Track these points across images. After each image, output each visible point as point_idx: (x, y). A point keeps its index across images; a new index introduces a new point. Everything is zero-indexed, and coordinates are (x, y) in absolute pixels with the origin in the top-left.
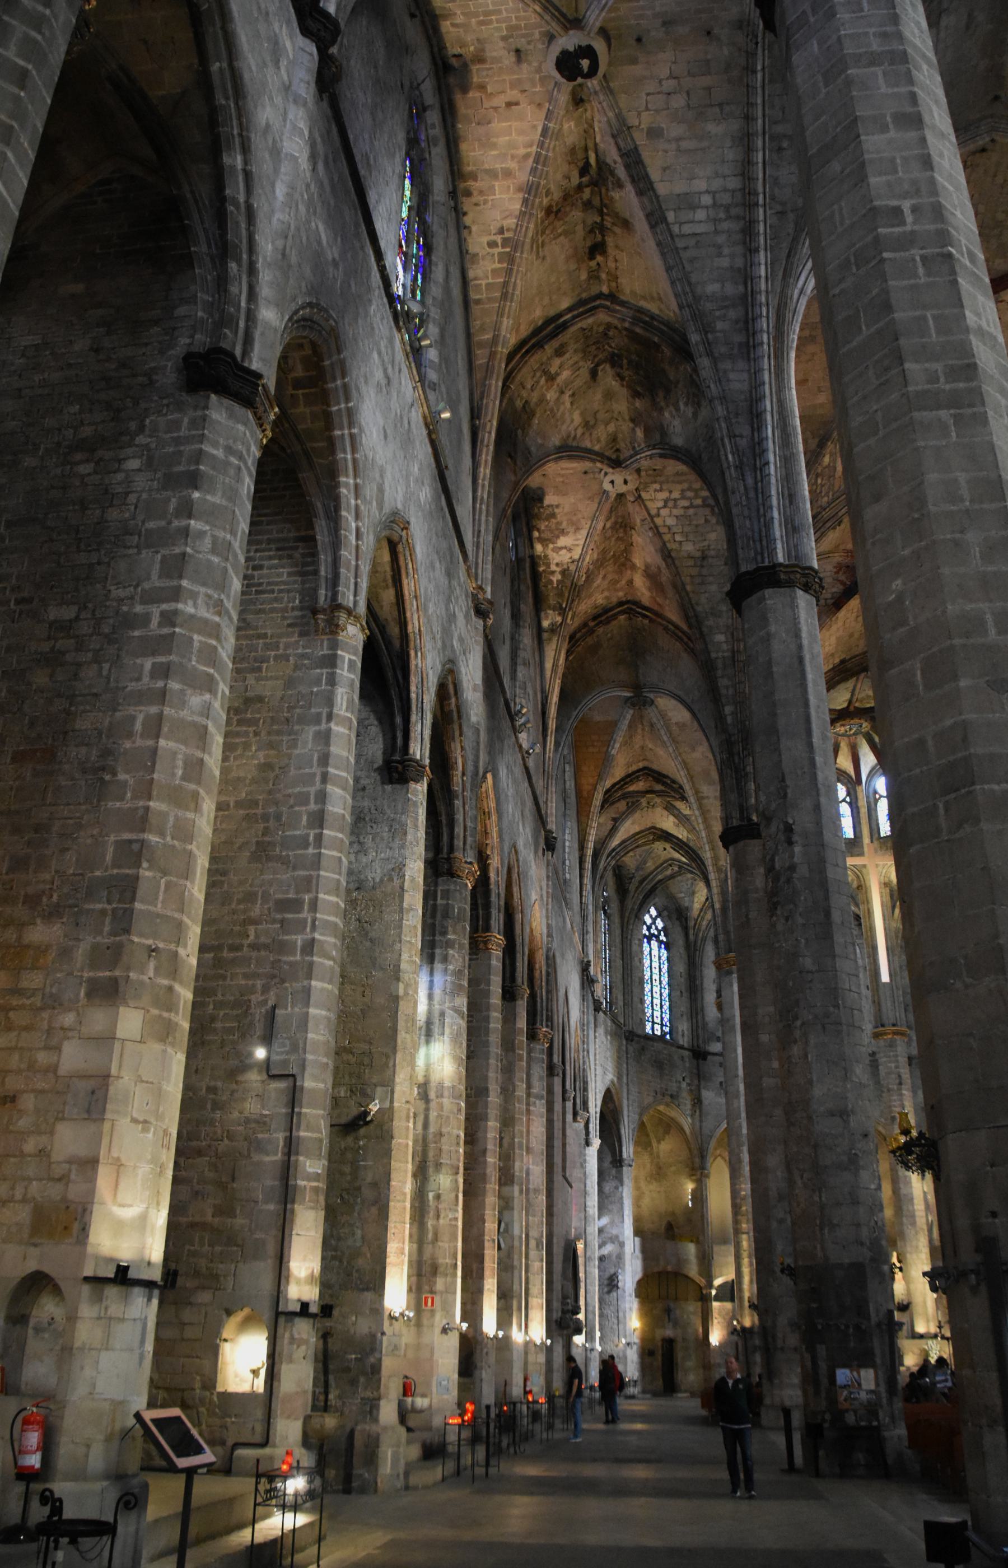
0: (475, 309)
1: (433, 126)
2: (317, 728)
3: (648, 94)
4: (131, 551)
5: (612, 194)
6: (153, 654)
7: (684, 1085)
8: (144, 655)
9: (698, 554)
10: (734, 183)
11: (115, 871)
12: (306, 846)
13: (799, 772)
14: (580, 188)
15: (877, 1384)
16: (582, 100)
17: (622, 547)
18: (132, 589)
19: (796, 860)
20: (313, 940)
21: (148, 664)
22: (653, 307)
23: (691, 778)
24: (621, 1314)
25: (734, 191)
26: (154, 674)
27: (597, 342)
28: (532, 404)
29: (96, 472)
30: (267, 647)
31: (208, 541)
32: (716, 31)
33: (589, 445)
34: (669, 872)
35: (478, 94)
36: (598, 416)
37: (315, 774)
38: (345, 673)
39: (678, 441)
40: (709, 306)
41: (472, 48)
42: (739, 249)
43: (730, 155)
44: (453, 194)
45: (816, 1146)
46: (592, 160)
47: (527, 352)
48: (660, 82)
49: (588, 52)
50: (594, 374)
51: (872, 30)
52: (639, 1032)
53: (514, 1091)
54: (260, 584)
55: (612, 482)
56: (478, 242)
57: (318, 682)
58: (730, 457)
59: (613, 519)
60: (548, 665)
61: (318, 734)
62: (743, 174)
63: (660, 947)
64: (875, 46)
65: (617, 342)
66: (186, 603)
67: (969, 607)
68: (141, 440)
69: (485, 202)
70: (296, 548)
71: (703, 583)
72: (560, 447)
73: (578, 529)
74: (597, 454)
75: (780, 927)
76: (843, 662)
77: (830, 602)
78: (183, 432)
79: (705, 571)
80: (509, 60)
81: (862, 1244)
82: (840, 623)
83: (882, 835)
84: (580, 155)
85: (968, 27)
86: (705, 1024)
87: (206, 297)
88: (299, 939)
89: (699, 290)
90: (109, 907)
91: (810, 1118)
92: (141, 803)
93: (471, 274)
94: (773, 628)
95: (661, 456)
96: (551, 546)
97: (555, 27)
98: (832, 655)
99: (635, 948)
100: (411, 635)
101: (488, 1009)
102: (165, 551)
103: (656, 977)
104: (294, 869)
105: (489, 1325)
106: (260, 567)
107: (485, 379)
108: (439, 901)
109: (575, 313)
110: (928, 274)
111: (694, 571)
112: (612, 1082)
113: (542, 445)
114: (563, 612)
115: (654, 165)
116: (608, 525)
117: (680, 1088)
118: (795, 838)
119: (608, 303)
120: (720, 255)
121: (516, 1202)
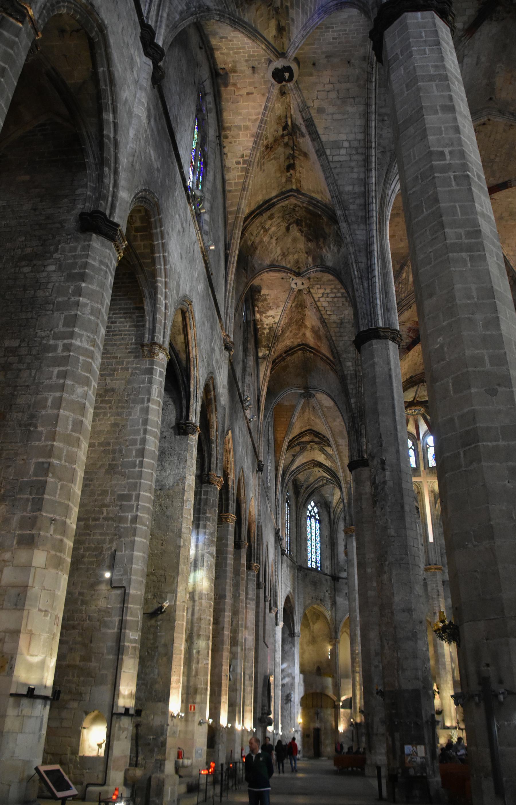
0: (229, 195)
1: (210, 103)
2: (142, 405)
3: (318, 91)
4: (49, 313)
5: (299, 140)
6: (58, 366)
7: (327, 594)
8: (54, 366)
9: (339, 321)
10: (360, 136)
11: (35, 478)
12: (135, 466)
13: (389, 433)
14: (283, 136)
15: (426, 753)
16: (285, 93)
17: (300, 317)
18: (48, 332)
19: (386, 478)
20: (137, 516)
21: (56, 370)
22: (318, 197)
23: (333, 435)
24: (292, 715)
25: (359, 141)
26: (58, 377)
27: (290, 213)
29: (32, 272)
30: (118, 363)
31: (89, 309)
32: (352, 61)
33: (284, 265)
34: (321, 483)
35: (232, 88)
36: (290, 250)
37: (140, 430)
38: (157, 378)
39: (330, 264)
40: (346, 197)
41: (230, 65)
42: (363, 169)
43: (358, 122)
44: (219, 137)
45: (395, 628)
46: (289, 123)
47: (254, 217)
48: (324, 85)
49: (289, 69)
50: (288, 229)
51: (430, 64)
52: (305, 566)
53: (239, 596)
54: (115, 331)
55: (296, 284)
56: (231, 161)
57: (143, 382)
58: (356, 273)
59: (296, 303)
60: (261, 375)
61: (142, 409)
62: (364, 132)
63: (316, 522)
64: (432, 72)
65: (300, 213)
66: (76, 340)
67: (476, 352)
68: (56, 256)
69: (235, 142)
70: (134, 313)
71: (340, 336)
72: (270, 266)
73: (278, 307)
74: (288, 269)
75: (378, 513)
76: (411, 377)
78: (78, 252)
79: (342, 330)
80: (249, 72)
81: (418, 679)
82: (410, 358)
83: (430, 466)
84: (283, 120)
85: (477, 64)
86: (338, 563)
87: (92, 185)
88: (130, 516)
89: (341, 189)
90: (31, 497)
91: (392, 613)
92: (50, 443)
93: (227, 177)
94: (376, 360)
95: (321, 271)
97: (272, 56)
98: (406, 374)
99: (303, 522)
100: (192, 359)
101: (227, 553)
102: (66, 313)
103: (313, 537)
104: (128, 479)
105: (224, 721)
106: (115, 322)
107: (233, 230)
108: (203, 497)
109: (279, 198)
110: (457, 184)
111: (337, 330)
112: (290, 592)
113: (261, 264)
114: (269, 348)
115: (320, 126)
116: (294, 305)
117: (325, 596)
118: (387, 467)
120: (352, 172)
121: (239, 655)
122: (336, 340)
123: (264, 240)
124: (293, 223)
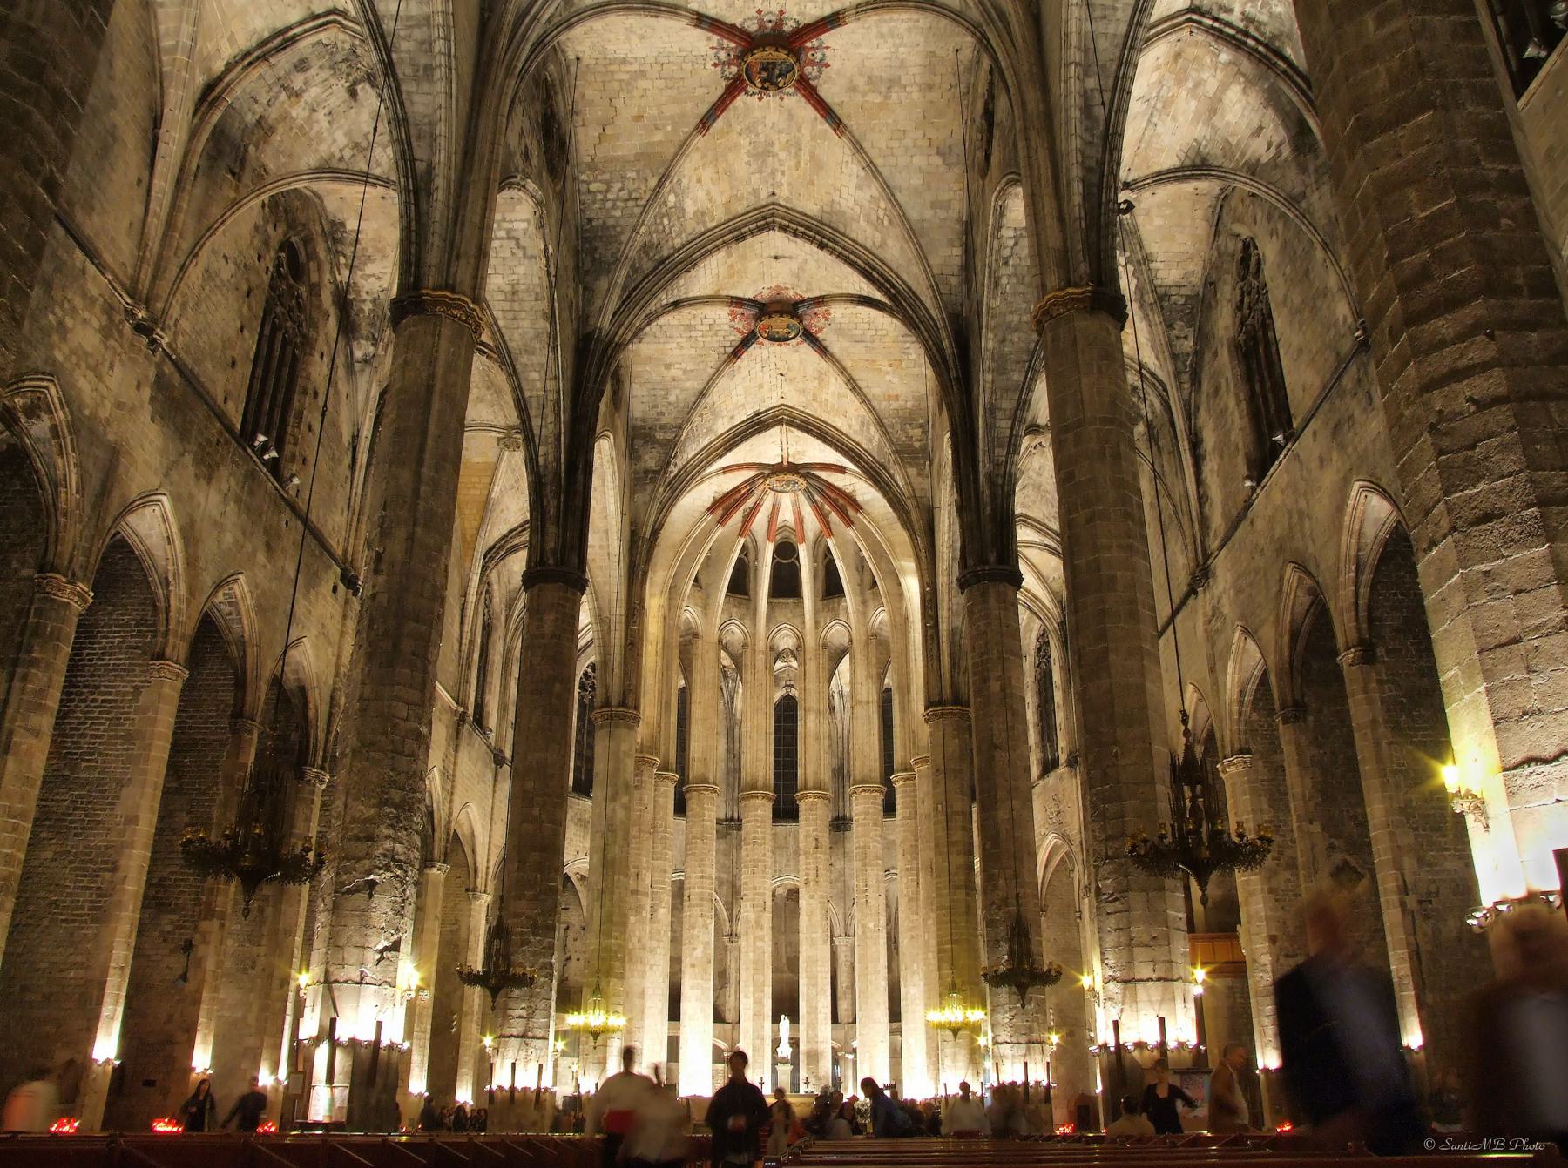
9: (508, 288)
27: (343, 61)
28: (270, 121)
47: (250, 64)
50: (353, 93)
60: (361, 397)
71: (514, 319)
73: (384, 257)
74: (377, 178)
76: (758, 414)
77: (730, 350)
79: (516, 306)
82: (744, 372)
96: (359, 273)
98: (743, 405)
111: (507, 306)
114: (375, 341)
118: (383, 567)
119: (340, 19)
122: (505, 327)
123: (294, 114)
124: (361, 81)
